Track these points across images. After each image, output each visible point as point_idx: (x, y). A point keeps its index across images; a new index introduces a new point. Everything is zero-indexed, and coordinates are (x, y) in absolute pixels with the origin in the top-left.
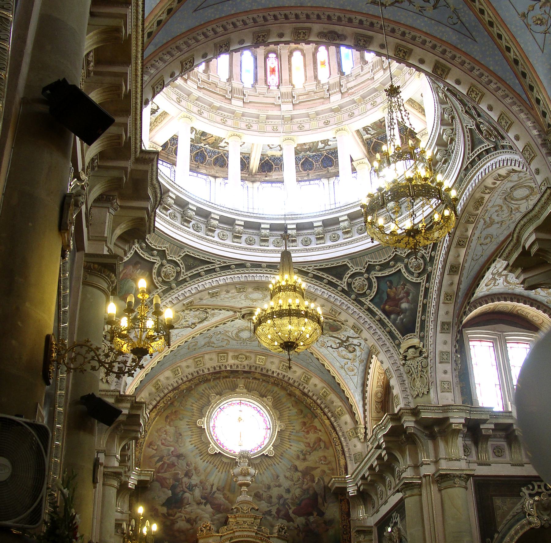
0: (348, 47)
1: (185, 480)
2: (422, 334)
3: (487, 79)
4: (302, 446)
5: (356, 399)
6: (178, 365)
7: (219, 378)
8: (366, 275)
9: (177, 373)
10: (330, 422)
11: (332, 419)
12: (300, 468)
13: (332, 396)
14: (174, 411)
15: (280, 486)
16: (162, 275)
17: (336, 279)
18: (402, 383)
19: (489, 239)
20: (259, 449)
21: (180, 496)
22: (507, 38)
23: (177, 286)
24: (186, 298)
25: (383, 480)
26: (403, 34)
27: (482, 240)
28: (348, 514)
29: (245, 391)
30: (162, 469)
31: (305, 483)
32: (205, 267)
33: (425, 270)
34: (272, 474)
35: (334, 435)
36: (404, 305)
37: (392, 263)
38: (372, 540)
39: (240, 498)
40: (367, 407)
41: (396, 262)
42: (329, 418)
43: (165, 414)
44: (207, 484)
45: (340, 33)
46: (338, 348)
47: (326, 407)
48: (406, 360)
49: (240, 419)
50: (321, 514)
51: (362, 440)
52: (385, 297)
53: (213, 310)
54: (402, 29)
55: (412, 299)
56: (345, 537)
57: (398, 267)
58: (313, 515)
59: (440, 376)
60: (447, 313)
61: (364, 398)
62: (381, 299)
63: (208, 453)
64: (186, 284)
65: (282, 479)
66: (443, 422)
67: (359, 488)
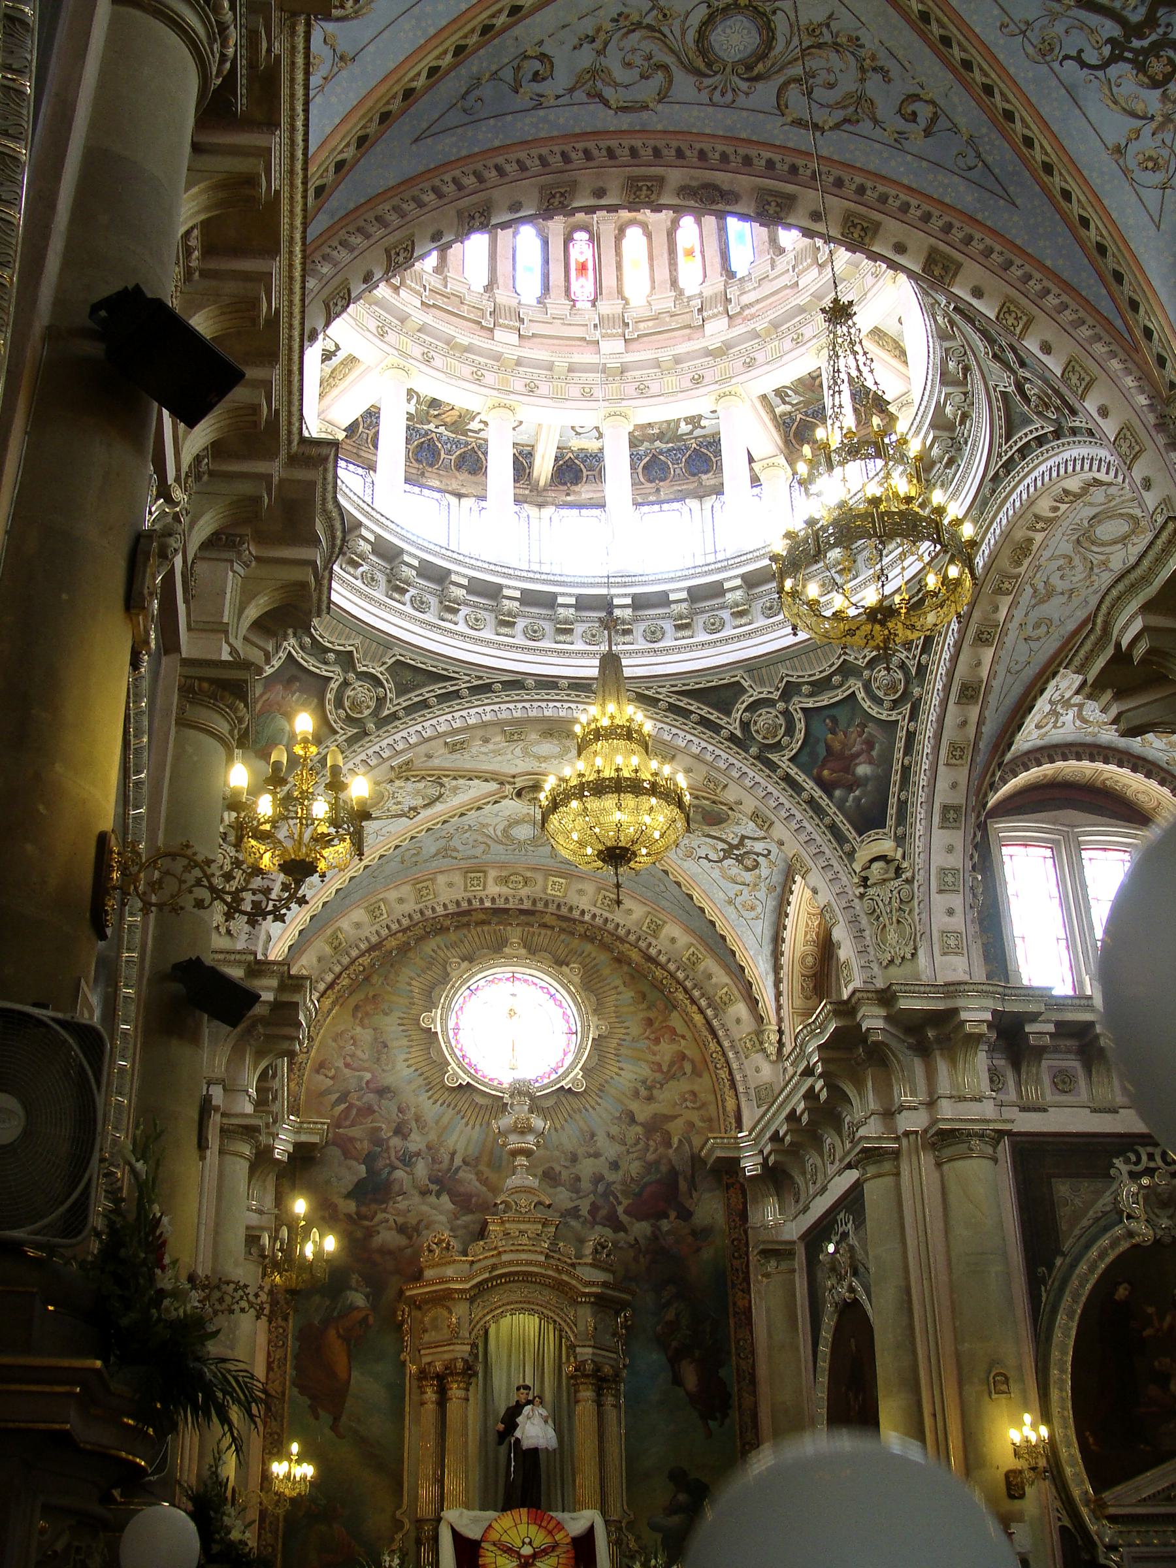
0: (743, 217)
1: (396, 1142)
2: (900, 830)
3: (1038, 287)
4: (645, 1071)
5: (759, 969)
7: (468, 925)
8: (781, 706)
9: (377, 913)
10: (705, 1018)
11: (709, 1012)
13: (709, 964)
15: (597, 1155)
16: (347, 704)
17: (716, 714)
18: (859, 935)
19: (1044, 629)
20: (553, 1076)
21: (384, 1175)
22: (1083, 198)
23: (378, 728)
24: (398, 753)
25: (817, 1142)
26: (861, 190)
27: (1029, 631)
28: (744, 1216)
29: (523, 951)
30: (346, 1118)
32: (439, 688)
33: (906, 694)
34: (581, 1130)
35: (713, 1046)
36: (863, 770)
37: (836, 679)
38: (794, 1271)
39: (513, 1181)
40: (783, 987)
41: (845, 678)
42: (701, 1011)
43: (353, 1001)
45: (725, 187)
46: (721, 861)
47: (695, 986)
48: (865, 886)
49: (512, 1013)
50: (686, 1215)
51: (774, 1058)
52: (822, 752)
53: (455, 778)
54: (858, 180)
55: (879, 756)
56: (737, 1263)
58: (667, 1217)
59: (940, 920)
60: (954, 786)
61: (777, 968)
62: (813, 755)
63: (444, 1086)
64: (397, 723)
65: (601, 1141)
66: (946, 1019)
67: (766, 1159)
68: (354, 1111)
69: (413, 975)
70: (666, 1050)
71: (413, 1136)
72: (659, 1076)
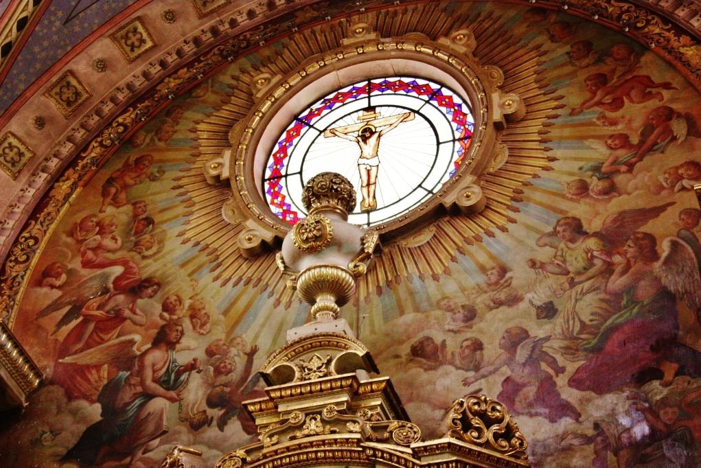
1: (157, 357)
4: (599, 152)
6: (139, 14)
9: (134, 39)
12: (595, 225)
14: (132, 159)
15: (514, 300)
30: (79, 339)
31: (618, 269)
34: (483, 269)
43: (106, 174)
44: (233, 351)
49: (366, 134)
65: (520, 274)
68: (91, 326)
69: (199, 116)
70: (635, 113)
71: (185, 342)
72: (623, 154)
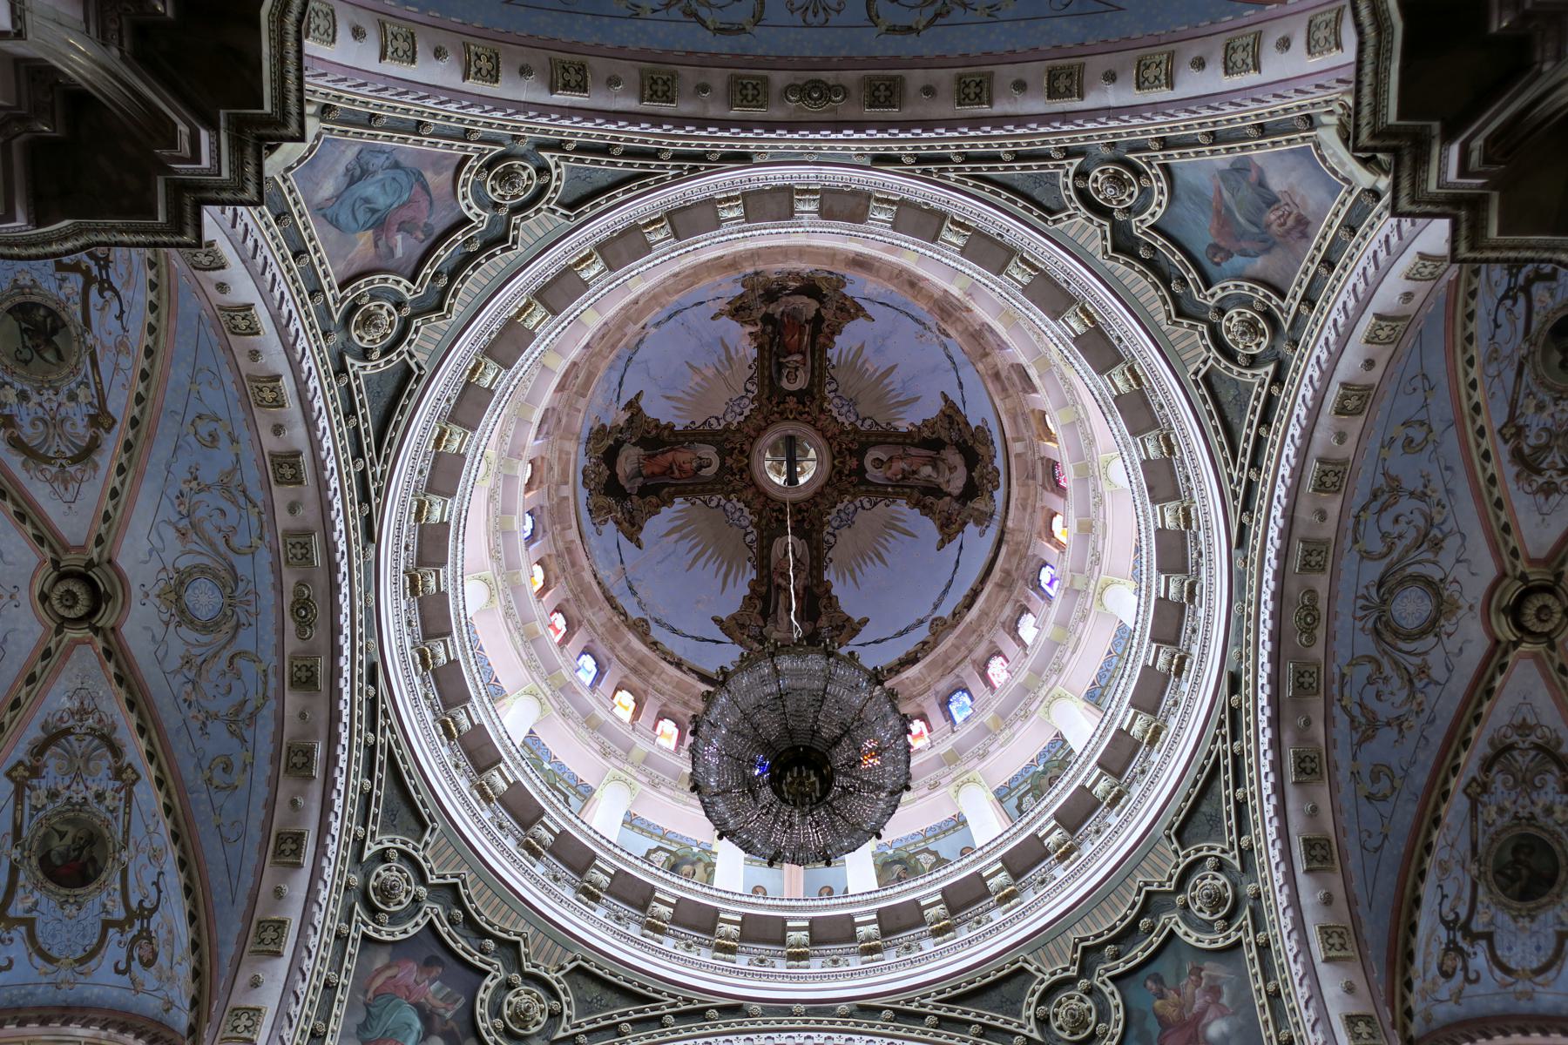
16: (506, 1012)
27: (1367, 786)
37: (1144, 923)
52: (1153, 1027)
55: (1233, 1000)
57: (1164, 927)
